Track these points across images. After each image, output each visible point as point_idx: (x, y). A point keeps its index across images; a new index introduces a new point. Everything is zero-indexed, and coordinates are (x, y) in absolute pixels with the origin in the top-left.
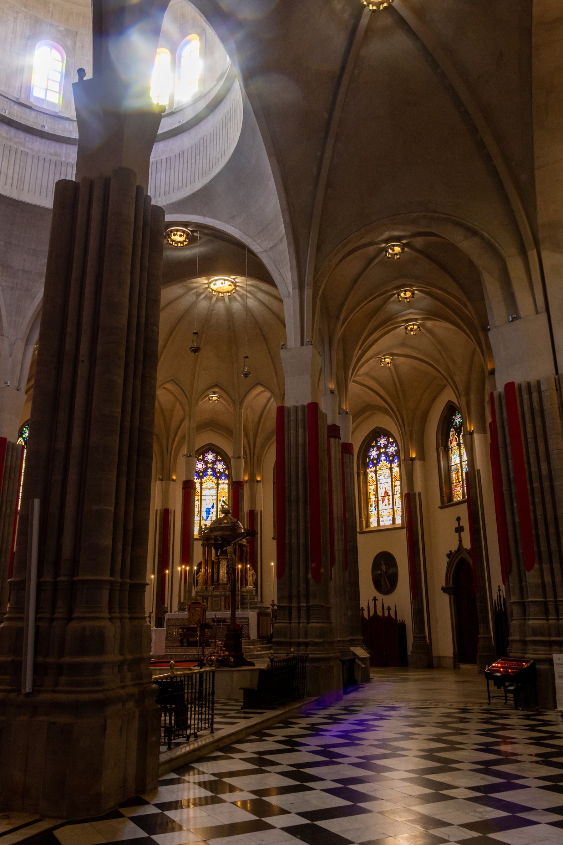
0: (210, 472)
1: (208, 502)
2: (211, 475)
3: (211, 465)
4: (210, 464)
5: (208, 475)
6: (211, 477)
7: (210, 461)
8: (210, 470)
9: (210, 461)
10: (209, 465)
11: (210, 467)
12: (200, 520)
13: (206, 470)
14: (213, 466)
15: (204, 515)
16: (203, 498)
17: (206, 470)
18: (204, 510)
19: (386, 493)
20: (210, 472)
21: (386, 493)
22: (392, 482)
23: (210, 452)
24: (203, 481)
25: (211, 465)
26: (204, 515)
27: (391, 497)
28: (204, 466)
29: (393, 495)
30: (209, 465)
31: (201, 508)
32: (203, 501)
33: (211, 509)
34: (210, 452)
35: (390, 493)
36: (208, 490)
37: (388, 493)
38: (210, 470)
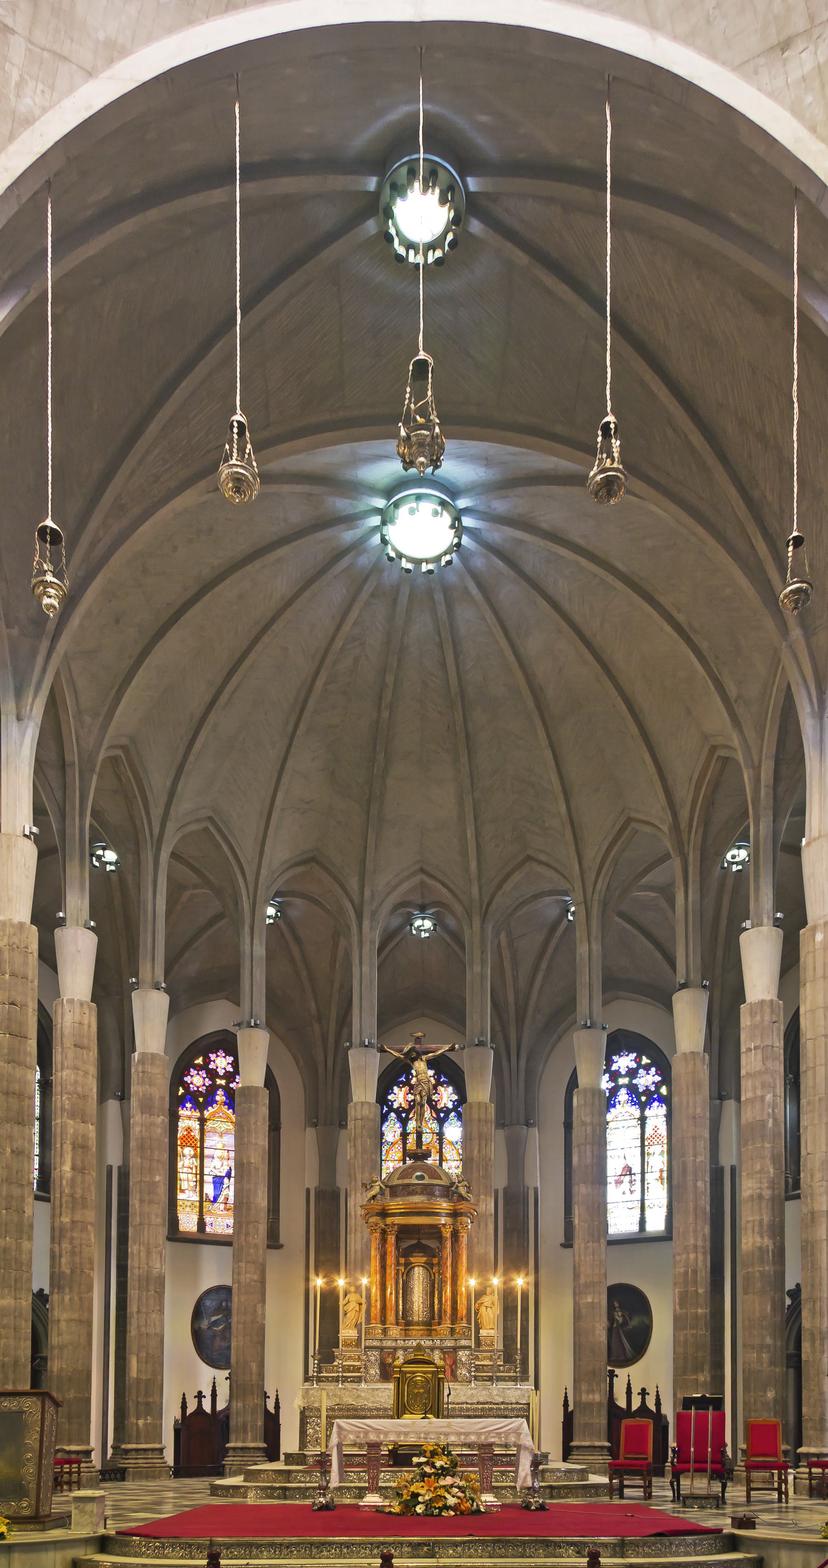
0: (220, 1097)
1: (217, 1163)
2: (225, 1103)
3: (223, 1082)
4: (221, 1078)
5: (216, 1102)
6: (225, 1108)
7: (221, 1072)
8: (220, 1092)
9: (221, 1072)
10: (219, 1082)
11: (221, 1086)
12: (201, 1202)
13: (212, 1090)
14: (228, 1083)
15: (209, 1190)
16: (207, 1152)
17: (212, 1090)
18: (208, 1179)
19: (628, 1171)
20: (220, 1097)
21: (628, 1171)
22: (643, 1146)
23: (221, 1053)
24: (206, 1114)
25: (223, 1082)
26: (209, 1190)
27: (638, 1177)
28: (208, 1082)
29: (643, 1173)
30: (219, 1082)
31: (202, 1174)
32: (206, 1160)
33: (226, 1180)
34: (221, 1053)
35: (637, 1169)
36: (216, 1138)
37: (630, 1169)
38: (220, 1092)
